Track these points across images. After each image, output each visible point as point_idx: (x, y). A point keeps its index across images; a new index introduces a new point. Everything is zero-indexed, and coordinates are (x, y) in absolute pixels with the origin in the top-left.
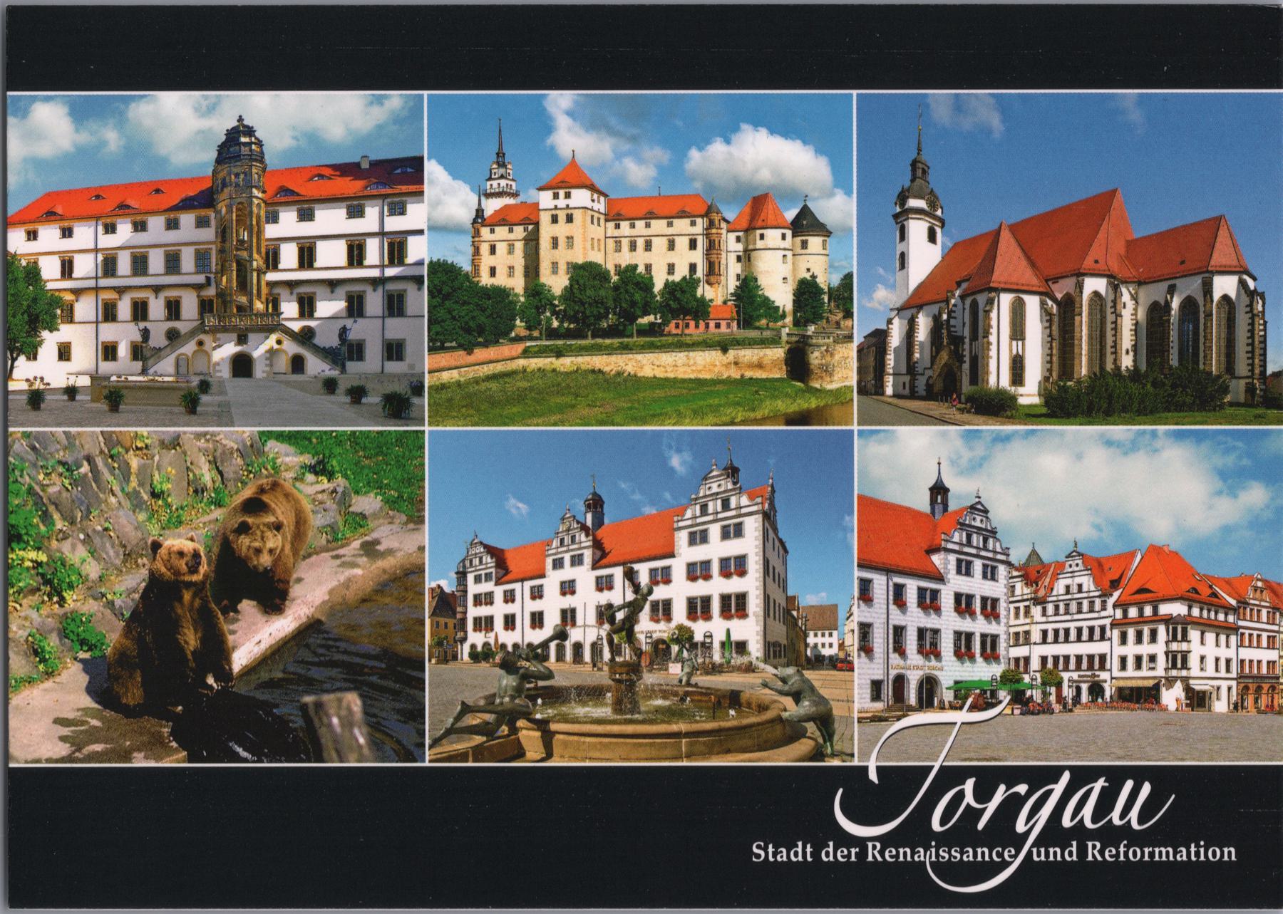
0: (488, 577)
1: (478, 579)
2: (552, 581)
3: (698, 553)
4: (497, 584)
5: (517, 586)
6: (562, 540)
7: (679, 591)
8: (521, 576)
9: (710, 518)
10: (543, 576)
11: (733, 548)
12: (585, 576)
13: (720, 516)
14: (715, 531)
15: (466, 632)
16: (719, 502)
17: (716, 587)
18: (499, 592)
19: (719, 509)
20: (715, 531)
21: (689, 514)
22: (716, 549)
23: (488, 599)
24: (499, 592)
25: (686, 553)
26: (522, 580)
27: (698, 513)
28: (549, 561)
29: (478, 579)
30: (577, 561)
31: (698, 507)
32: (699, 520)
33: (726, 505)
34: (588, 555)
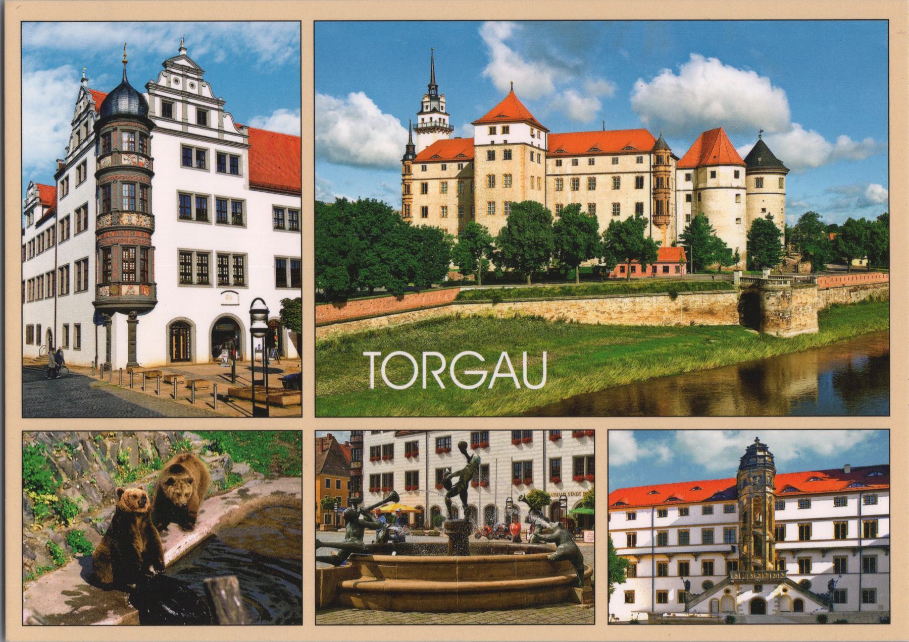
0: (227, 165)
1: (191, 158)
4: (254, 186)
29: (191, 158)
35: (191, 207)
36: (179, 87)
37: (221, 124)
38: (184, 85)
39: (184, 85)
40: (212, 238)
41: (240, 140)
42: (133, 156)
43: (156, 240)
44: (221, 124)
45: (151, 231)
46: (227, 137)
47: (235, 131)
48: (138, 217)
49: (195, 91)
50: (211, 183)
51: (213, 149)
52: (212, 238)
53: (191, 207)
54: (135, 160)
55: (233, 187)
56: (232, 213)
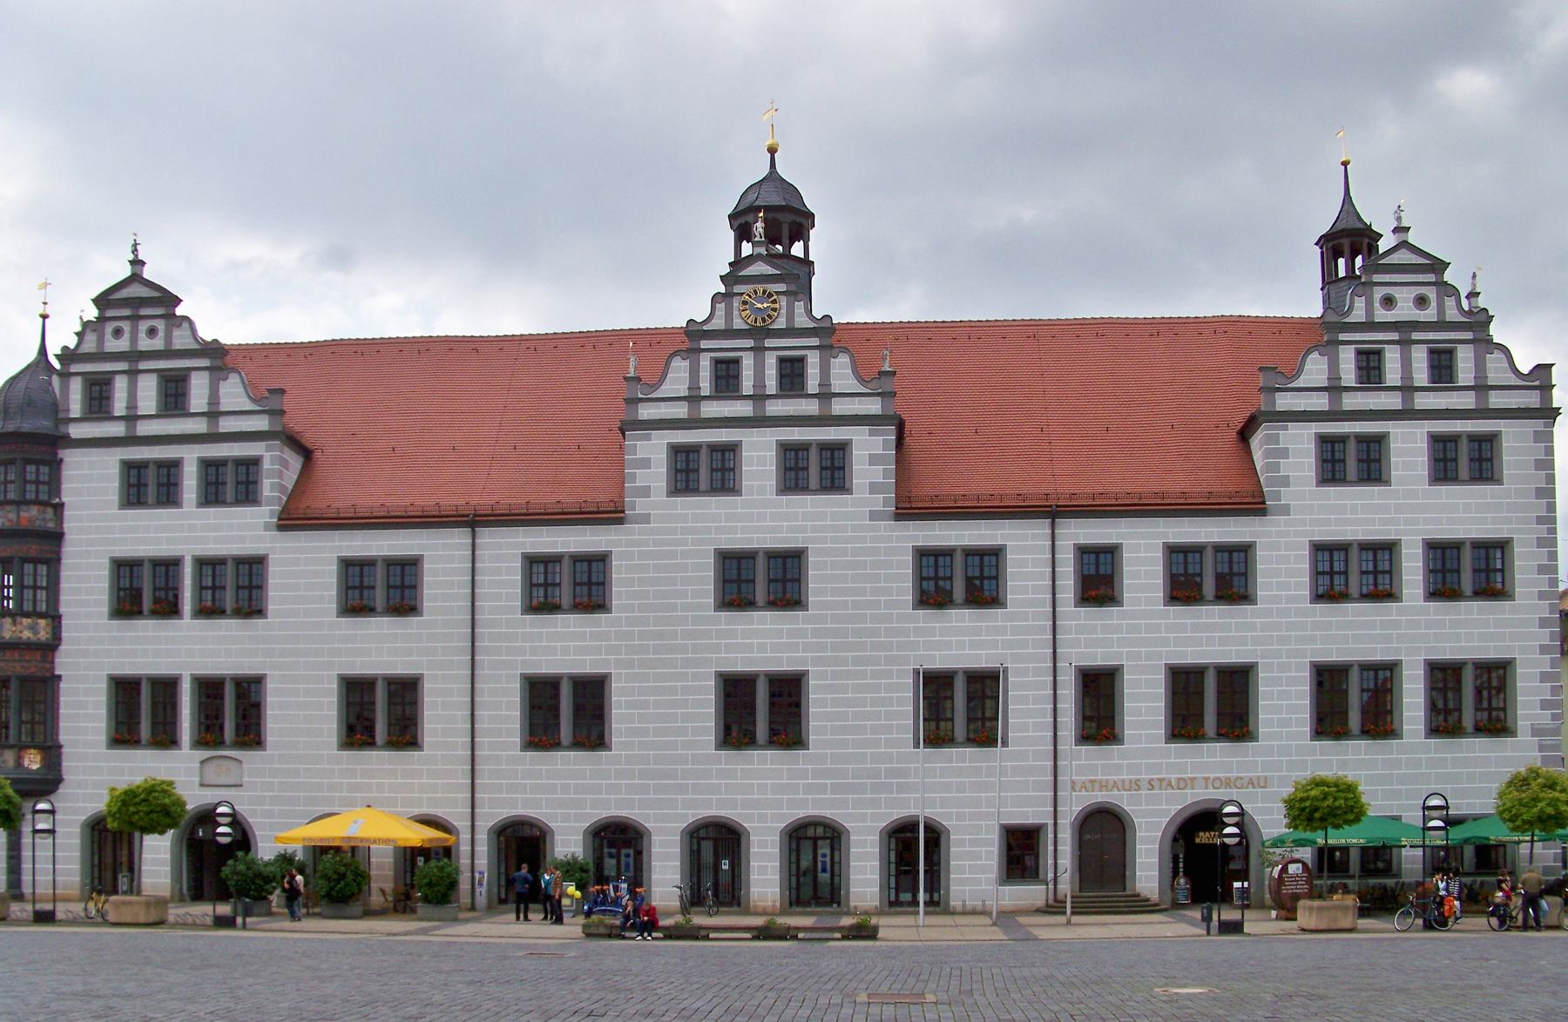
0: (229, 484)
1: (148, 486)
2: (666, 545)
3: (1354, 513)
4: (292, 519)
5: (440, 554)
6: (727, 377)
7: (1282, 635)
8: (481, 499)
9: (1393, 401)
10: (612, 515)
11: (1465, 513)
12: (856, 543)
13: (1423, 401)
14: (1408, 447)
15: (52, 752)
16: (1420, 357)
17: (1412, 632)
18: (304, 569)
19: (1421, 376)
20: (1408, 447)
21: (1315, 370)
22: (1410, 508)
23: (236, 588)
24: (304, 569)
25: (1309, 505)
26: (473, 521)
27: (1349, 375)
28: (651, 456)
29: (148, 486)
30: (815, 469)
31: (1347, 357)
32: (1351, 402)
33: (1442, 367)
34: (869, 454)
35: (142, 590)
36: (122, 345)
37: (214, 398)
38: (134, 339)
39: (134, 339)
40: (187, 648)
41: (261, 424)
42: (8, 508)
43: (64, 663)
44: (214, 398)
45: (50, 648)
46: (226, 425)
47: (249, 406)
48: (14, 623)
49: (158, 344)
50: (191, 531)
51: (190, 458)
52: (187, 648)
53: (142, 590)
54: (13, 516)
55: (236, 530)
56: (236, 588)
